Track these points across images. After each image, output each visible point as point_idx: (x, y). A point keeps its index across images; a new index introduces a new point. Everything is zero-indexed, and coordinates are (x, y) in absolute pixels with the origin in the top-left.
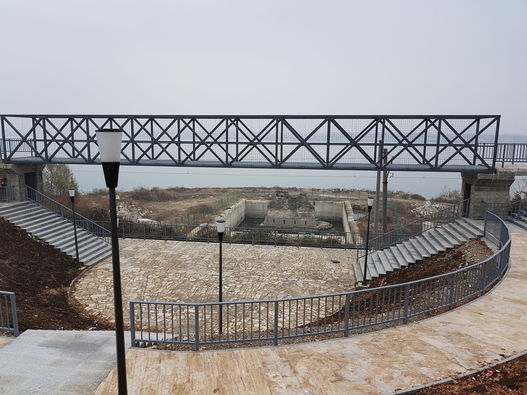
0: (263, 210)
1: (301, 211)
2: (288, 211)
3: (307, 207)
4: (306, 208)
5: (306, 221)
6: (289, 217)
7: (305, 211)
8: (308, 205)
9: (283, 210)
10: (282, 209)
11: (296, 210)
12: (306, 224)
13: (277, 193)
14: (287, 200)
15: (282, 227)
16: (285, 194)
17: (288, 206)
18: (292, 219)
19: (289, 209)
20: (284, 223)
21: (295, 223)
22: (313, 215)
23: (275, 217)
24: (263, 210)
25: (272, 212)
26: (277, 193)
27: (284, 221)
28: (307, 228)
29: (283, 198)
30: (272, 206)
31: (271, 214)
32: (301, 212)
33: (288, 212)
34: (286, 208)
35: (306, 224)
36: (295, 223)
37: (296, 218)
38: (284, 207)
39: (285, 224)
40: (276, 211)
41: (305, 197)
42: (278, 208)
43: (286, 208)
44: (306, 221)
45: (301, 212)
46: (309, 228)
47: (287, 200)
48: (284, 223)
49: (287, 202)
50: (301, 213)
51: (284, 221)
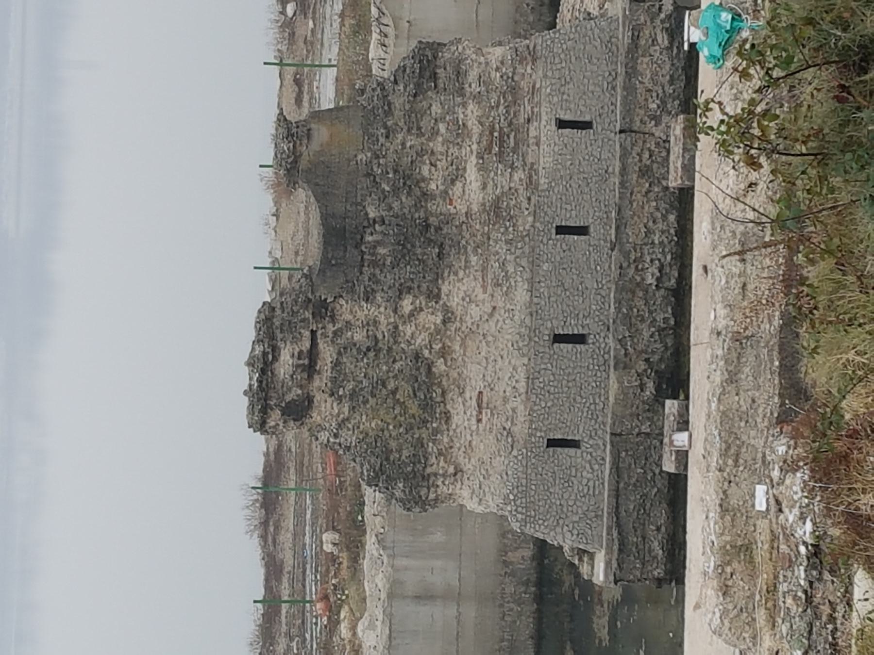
0: (455, 596)
1: (456, 175)
2: (455, 302)
3: (414, 126)
4: (426, 124)
5: (562, 124)
6: (521, 295)
7: (460, 131)
8: (399, 101)
9: (444, 353)
10: (440, 366)
11: (449, 219)
12: (586, 125)
13: (275, 418)
14: (345, 309)
15: (623, 365)
16: (289, 327)
17: (407, 305)
18: (534, 264)
19: (434, 296)
20: (580, 339)
21: (582, 231)
22: (499, 51)
23: (520, 429)
24: (455, 596)
25: (468, 466)
26: (275, 418)
27: (558, 339)
28: (628, 112)
29: (327, 353)
30: (415, 459)
31: (495, 478)
32: (472, 174)
33: (468, 298)
34: (431, 319)
35: (586, 125)
36: (582, 231)
37: (526, 222)
38: (421, 339)
39: (590, 326)
40: (456, 420)
41: (321, 133)
42: (427, 405)
43: (431, 319)
44: (562, 124)
45: (472, 174)
46: (629, 89)
47: (345, 309)
48: (580, 339)
49: (365, 311)
50: (482, 168)
51: (558, 339)
